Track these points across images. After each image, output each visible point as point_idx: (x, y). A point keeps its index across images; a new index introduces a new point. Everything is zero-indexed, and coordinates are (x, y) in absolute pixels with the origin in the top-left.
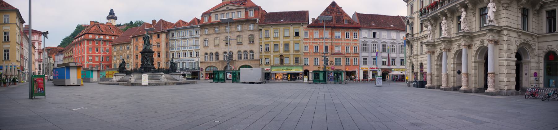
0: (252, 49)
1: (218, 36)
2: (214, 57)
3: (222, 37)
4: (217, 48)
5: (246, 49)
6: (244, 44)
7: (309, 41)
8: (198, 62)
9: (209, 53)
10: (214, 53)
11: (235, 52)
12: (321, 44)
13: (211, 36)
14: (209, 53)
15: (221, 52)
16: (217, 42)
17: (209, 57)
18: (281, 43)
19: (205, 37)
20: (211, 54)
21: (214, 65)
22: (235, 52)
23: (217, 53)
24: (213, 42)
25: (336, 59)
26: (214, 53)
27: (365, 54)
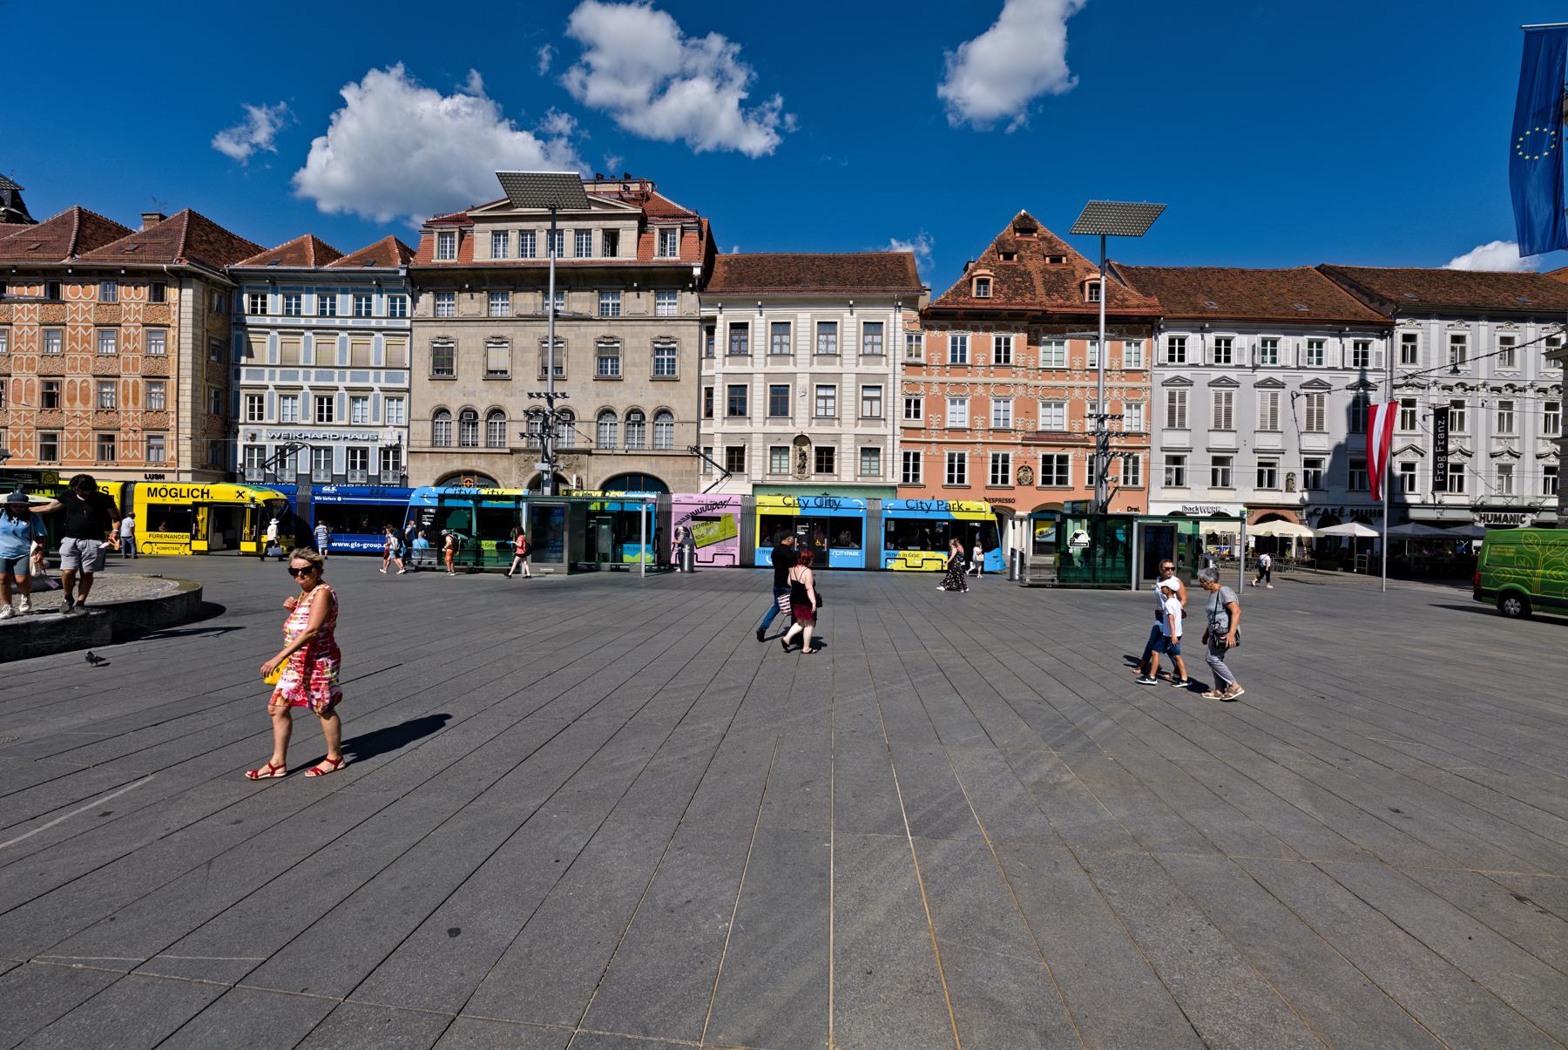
0: (665, 402)
1: (505, 331)
2: (482, 426)
3: (527, 338)
4: (498, 386)
5: (638, 402)
6: (628, 379)
7: (924, 377)
8: (397, 449)
9: (455, 408)
10: (482, 411)
11: (586, 411)
12: (980, 389)
13: (471, 330)
14: (455, 408)
15: (516, 406)
16: (499, 359)
17: (455, 426)
18: (803, 382)
19: (440, 332)
20: (469, 417)
21: (480, 465)
22: (586, 411)
23: (496, 412)
24: (478, 358)
25: (1047, 459)
26: (482, 411)
27: (1176, 439)
